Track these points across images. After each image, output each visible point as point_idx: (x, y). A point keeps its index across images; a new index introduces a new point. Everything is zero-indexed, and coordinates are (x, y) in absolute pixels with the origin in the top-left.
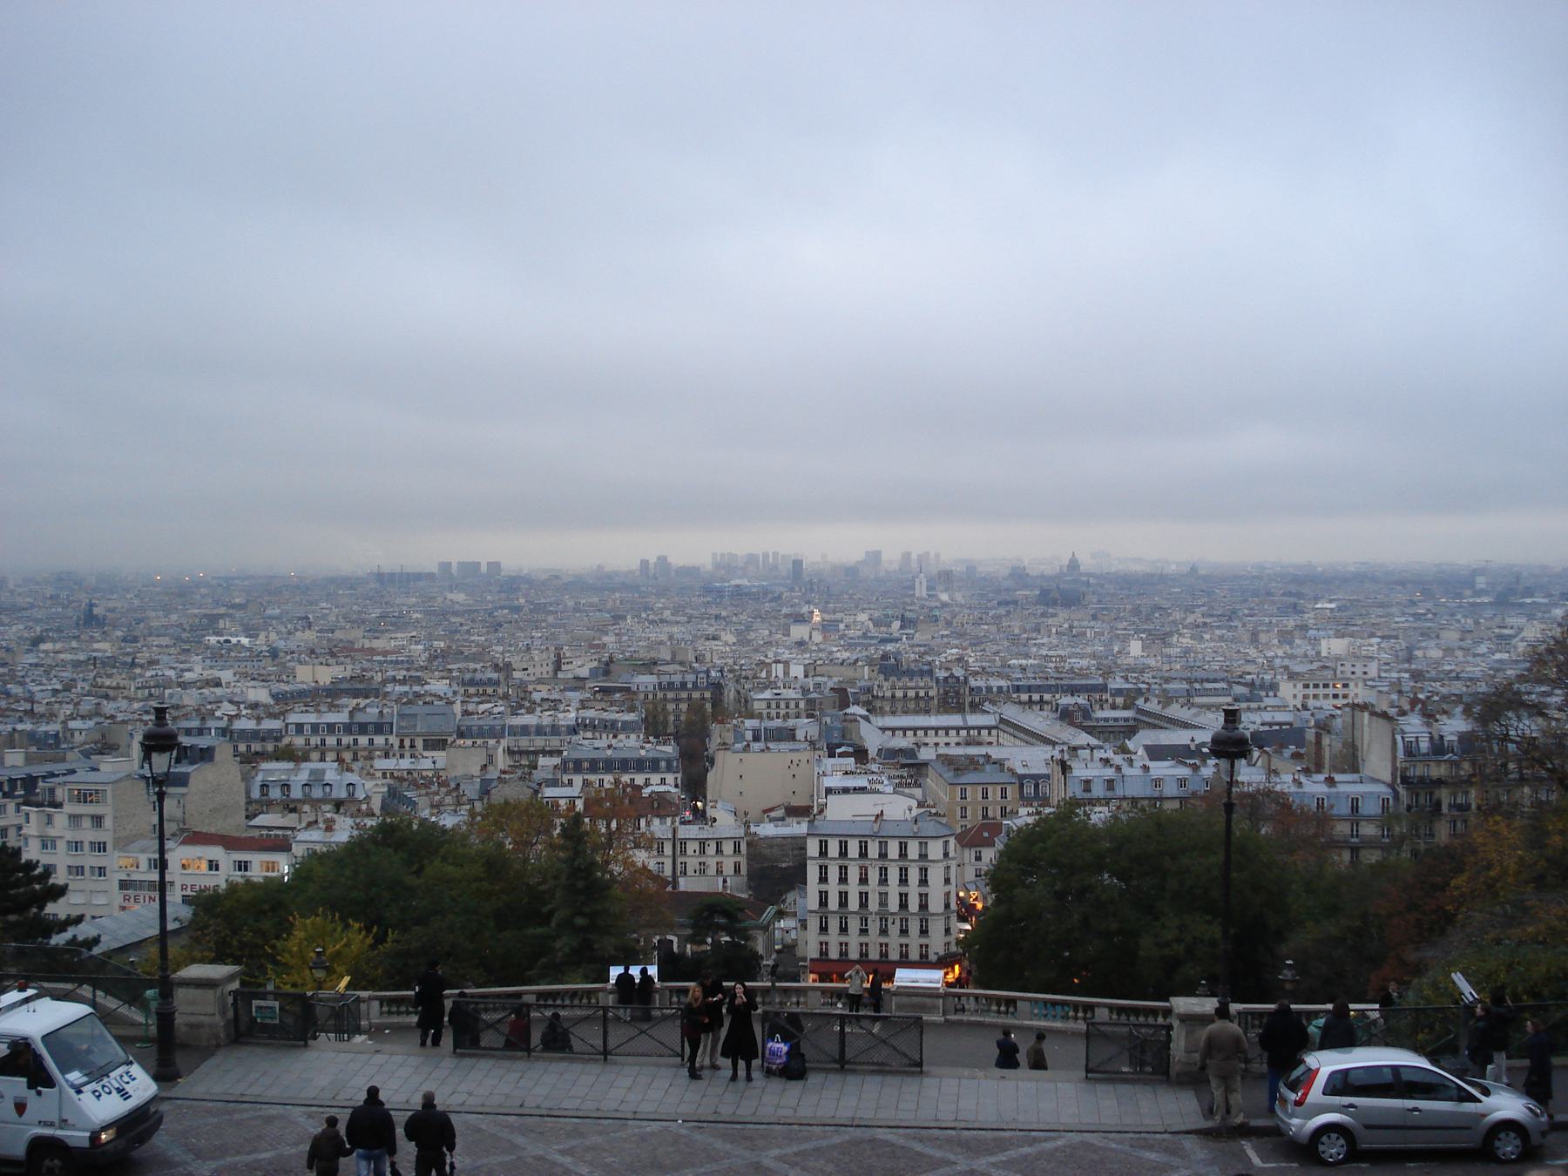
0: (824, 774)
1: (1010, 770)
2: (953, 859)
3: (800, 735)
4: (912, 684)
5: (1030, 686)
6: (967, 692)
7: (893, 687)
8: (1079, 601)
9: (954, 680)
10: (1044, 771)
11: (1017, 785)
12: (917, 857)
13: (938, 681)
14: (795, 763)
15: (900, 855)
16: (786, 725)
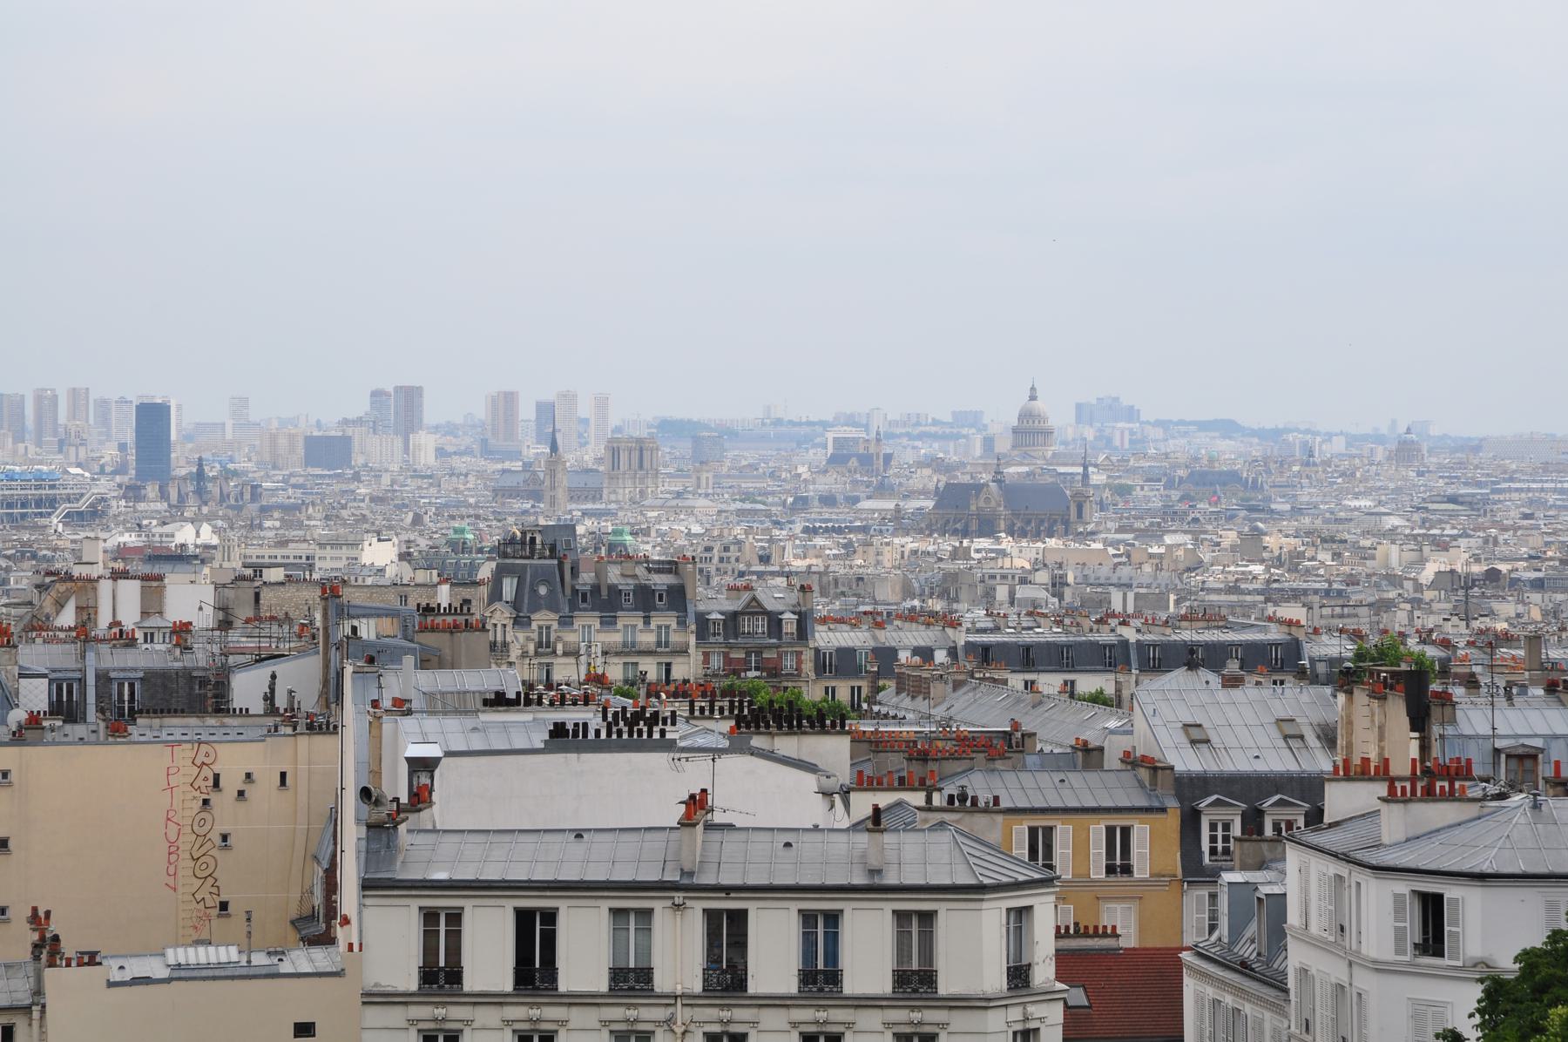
0: (402, 707)
1: (1131, 761)
2: (1048, 996)
3: (247, 688)
4: (615, 638)
5: (1027, 648)
6: (808, 667)
7: (545, 646)
8: (1066, 523)
9: (761, 625)
10: (1278, 761)
11: (1171, 822)
12: (885, 986)
13: (703, 623)
14: (231, 783)
15: (808, 976)
16: (187, 661)
